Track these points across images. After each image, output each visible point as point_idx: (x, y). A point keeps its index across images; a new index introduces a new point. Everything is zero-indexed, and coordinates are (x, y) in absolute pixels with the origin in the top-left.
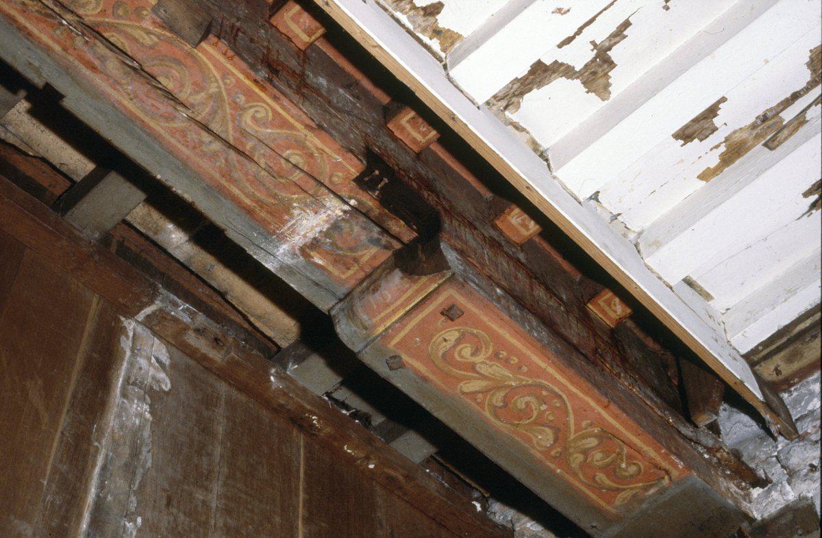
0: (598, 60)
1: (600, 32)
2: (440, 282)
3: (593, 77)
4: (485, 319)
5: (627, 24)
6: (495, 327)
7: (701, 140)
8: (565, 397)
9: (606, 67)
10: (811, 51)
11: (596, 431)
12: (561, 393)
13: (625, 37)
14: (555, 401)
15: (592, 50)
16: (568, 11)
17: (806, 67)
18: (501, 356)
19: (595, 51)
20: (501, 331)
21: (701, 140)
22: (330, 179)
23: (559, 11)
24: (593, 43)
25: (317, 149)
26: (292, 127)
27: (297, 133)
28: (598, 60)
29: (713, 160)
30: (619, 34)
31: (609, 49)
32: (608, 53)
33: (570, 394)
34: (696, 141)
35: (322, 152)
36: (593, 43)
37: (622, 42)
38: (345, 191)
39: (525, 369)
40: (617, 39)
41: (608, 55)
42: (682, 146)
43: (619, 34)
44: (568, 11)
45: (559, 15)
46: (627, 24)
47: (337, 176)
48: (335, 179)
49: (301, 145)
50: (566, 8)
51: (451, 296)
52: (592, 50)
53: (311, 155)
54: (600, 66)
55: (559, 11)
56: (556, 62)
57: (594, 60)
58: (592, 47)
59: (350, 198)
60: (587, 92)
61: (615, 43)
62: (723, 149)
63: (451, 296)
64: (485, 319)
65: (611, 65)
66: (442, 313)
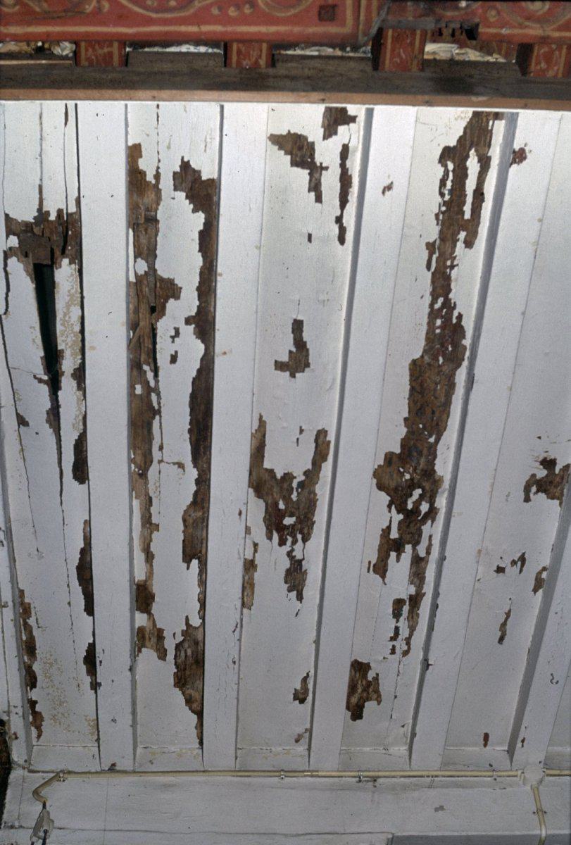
0: (309, 160)
1: (330, 182)
2: (361, 27)
3: (298, 144)
4: (297, 29)
5: (319, 199)
6: (282, 29)
7: (175, 173)
8: (154, 15)
9: (298, 159)
10: (181, 288)
11: (87, 7)
12: (160, 15)
13: (309, 190)
14: (155, 4)
15: (321, 164)
16: (383, 193)
17: (171, 277)
18: (247, 6)
19: (318, 164)
20: (273, 29)
21: (175, 173)
22: (496, 9)
23: (389, 187)
24: (326, 168)
25: (526, 27)
26: (559, 29)
27: (552, 27)
28: (309, 160)
29: (146, 165)
30: (315, 187)
31: (310, 174)
32: (308, 171)
33: (150, 21)
34: (178, 169)
35: (521, 26)
36: (326, 168)
37: (307, 186)
38: (477, 9)
39: (215, 11)
40: (313, 184)
41: (307, 169)
42: (183, 158)
43: (315, 187)
44: (383, 193)
45: (387, 183)
46: (319, 199)
47: (494, 17)
48: (493, 13)
49: (542, 20)
50: (387, 193)
51: (343, 24)
52: (321, 164)
53: (528, 19)
54: (303, 157)
55: (389, 187)
56: (336, 133)
57: (312, 156)
58: (324, 165)
59: (467, 6)
60: (289, 131)
61: (310, 181)
62: (150, 178)
63: (343, 24)
64: (297, 29)
65: (294, 163)
66: (334, 7)
